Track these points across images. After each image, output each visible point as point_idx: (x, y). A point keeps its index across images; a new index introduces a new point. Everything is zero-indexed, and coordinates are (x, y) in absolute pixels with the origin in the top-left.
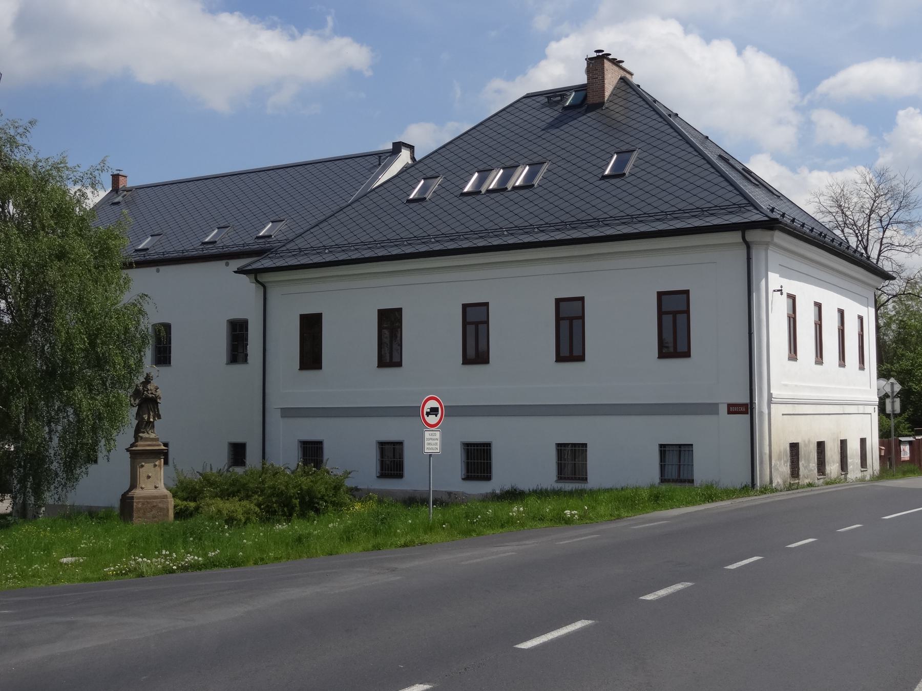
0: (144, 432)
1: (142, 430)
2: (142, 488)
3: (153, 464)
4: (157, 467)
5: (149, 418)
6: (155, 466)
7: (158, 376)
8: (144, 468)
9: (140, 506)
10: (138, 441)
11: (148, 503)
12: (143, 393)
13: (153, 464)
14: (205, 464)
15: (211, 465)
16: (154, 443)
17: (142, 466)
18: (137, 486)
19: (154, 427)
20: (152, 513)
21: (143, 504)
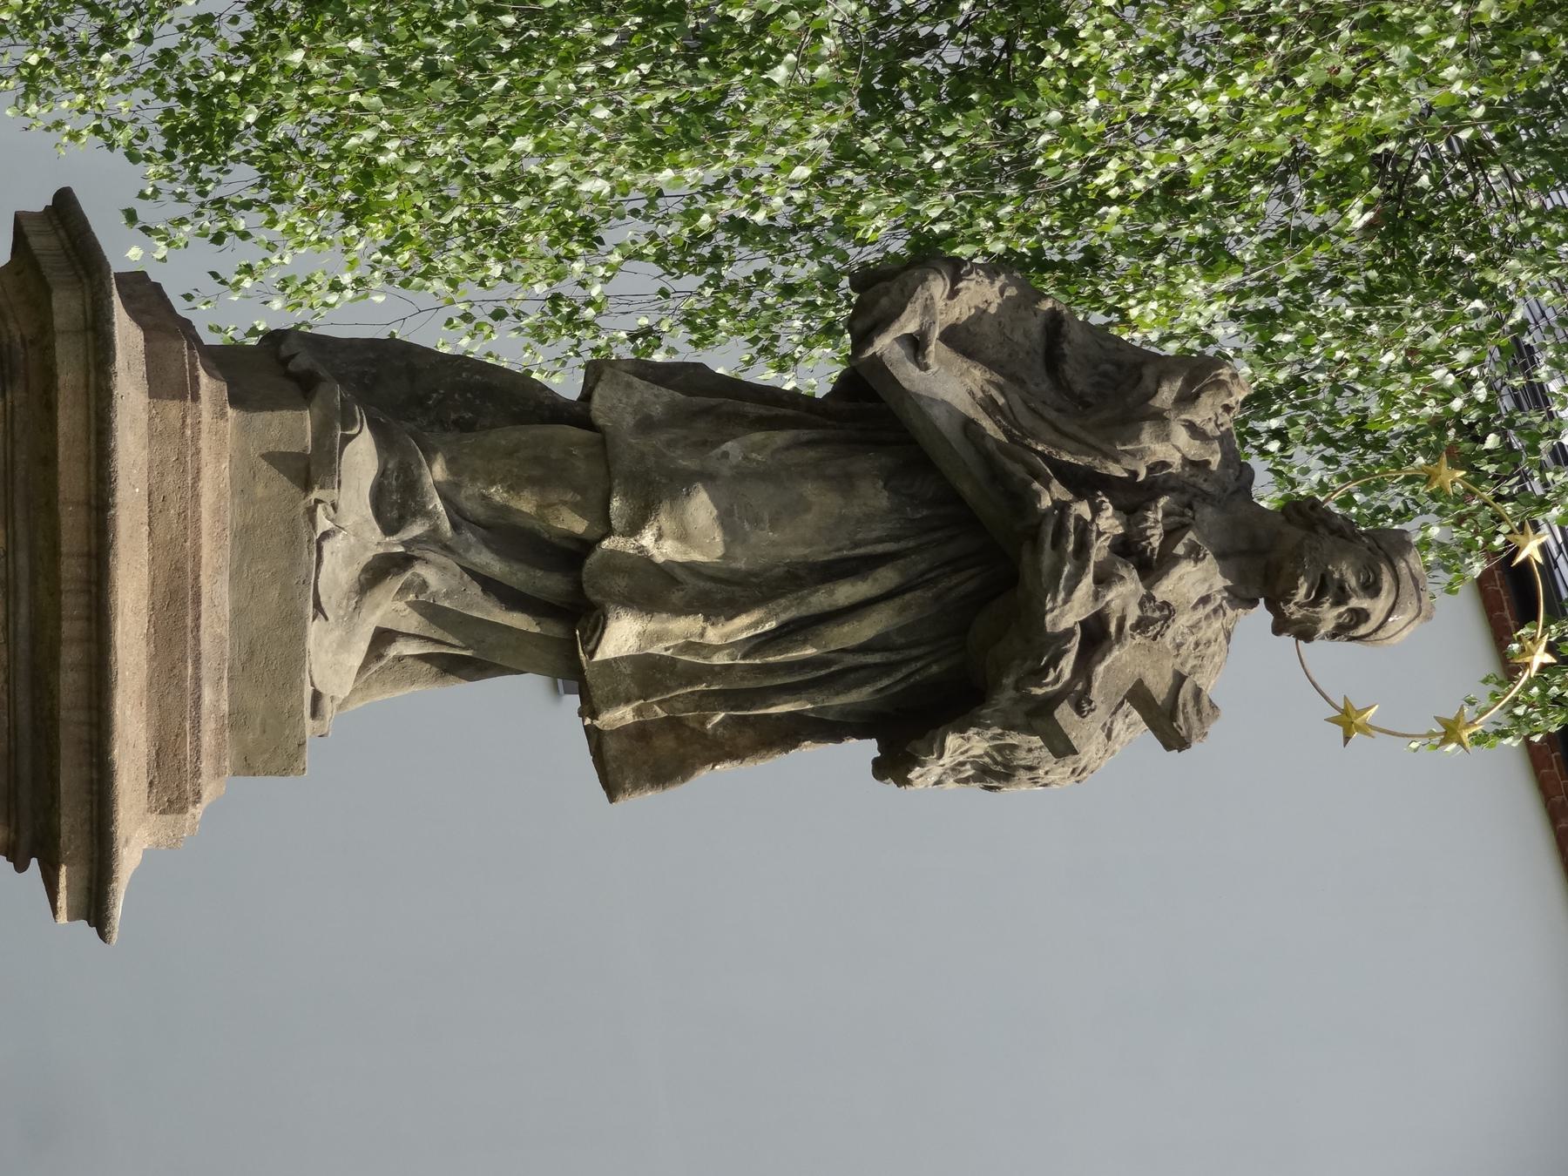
1: (436, 472)
7: (1347, 721)
10: (236, 400)
12: (1085, 483)
16: (214, 699)
19: (451, 667)
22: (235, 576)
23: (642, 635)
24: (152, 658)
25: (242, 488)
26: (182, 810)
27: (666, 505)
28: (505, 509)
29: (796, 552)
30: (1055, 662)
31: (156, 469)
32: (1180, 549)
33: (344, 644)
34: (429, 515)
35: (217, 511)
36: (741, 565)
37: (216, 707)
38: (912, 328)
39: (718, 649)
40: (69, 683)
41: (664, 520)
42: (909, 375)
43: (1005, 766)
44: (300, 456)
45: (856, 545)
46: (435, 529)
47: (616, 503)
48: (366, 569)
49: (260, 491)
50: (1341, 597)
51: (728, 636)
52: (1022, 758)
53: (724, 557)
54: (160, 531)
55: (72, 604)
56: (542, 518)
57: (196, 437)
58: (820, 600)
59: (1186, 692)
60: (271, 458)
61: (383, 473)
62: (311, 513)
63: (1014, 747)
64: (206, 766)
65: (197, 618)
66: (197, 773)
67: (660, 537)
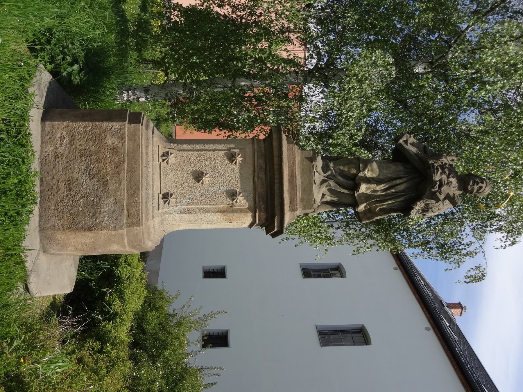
0: (325, 169)
2: (166, 155)
3: (237, 186)
4: (228, 200)
5: (368, 181)
6: (233, 195)
8: (226, 161)
9: (110, 141)
11: (118, 165)
13: (237, 186)
14: (216, 371)
15: (215, 383)
16: (299, 195)
17: (232, 157)
18: (170, 143)
20: (84, 179)
21: (115, 151)
22: (301, 177)
23: (366, 188)
24: (289, 186)
25: (302, 162)
26: (295, 211)
27: (369, 164)
28: (343, 171)
29: (390, 175)
30: (436, 185)
31: (289, 155)
32: (450, 176)
33: (318, 193)
34: (331, 170)
35: (298, 164)
36: (381, 177)
37: (299, 196)
38: (405, 139)
39: (378, 191)
40: (276, 186)
41: (369, 167)
42: (405, 146)
43: (427, 209)
44: (311, 158)
45: (399, 175)
46: (332, 172)
47: (361, 165)
48: (321, 182)
49: (305, 163)
50: (478, 184)
51: (380, 188)
52: (431, 206)
53: (379, 175)
54: (289, 165)
55: (276, 173)
56: (349, 171)
57: (295, 151)
58: (394, 182)
59: (455, 196)
60: (306, 158)
61: (323, 165)
62: (313, 166)
63: (428, 204)
64: (298, 207)
65: (296, 180)
66: (297, 206)
67: (368, 171)
